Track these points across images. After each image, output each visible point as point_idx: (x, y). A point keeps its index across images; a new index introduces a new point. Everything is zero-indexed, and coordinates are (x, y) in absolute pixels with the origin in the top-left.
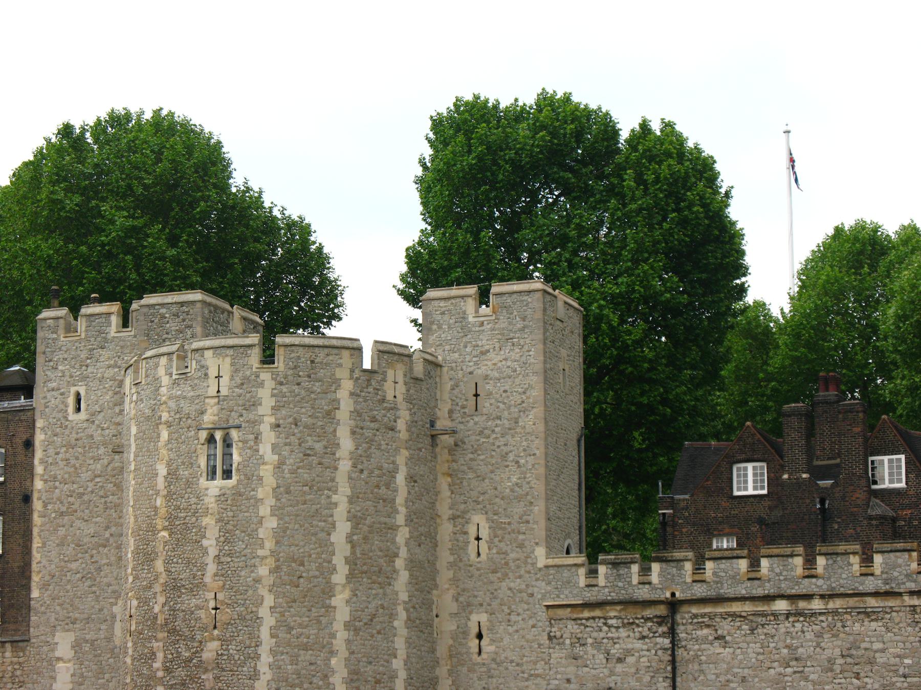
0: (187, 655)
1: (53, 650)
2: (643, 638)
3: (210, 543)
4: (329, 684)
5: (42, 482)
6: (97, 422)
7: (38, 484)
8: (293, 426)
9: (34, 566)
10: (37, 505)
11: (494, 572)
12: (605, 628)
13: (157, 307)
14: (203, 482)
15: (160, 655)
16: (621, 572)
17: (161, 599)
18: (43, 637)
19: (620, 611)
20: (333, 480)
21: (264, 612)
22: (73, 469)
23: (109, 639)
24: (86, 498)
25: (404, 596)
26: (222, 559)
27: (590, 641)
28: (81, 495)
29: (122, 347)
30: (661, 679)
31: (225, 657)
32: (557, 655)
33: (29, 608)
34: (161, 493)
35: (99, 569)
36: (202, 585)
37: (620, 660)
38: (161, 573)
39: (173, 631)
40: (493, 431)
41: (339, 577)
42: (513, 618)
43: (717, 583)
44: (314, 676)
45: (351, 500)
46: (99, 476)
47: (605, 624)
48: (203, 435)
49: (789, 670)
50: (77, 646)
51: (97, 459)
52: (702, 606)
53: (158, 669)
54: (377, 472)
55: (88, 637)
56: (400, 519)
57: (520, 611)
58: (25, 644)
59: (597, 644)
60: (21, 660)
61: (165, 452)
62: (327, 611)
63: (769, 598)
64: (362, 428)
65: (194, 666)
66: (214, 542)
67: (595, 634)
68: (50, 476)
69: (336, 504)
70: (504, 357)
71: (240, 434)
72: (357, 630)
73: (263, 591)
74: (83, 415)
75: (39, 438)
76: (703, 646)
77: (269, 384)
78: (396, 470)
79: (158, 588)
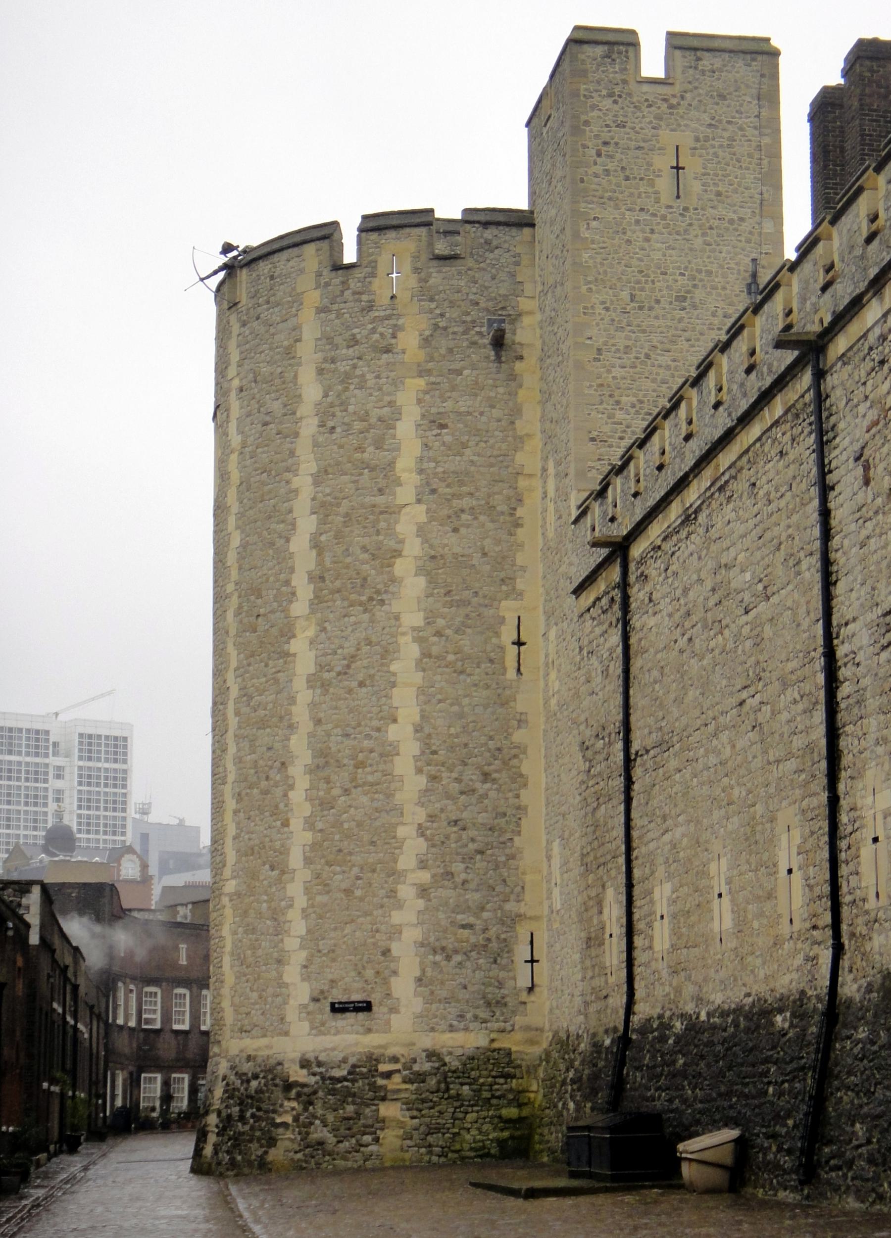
4: (287, 777)
8: (253, 384)
20: (292, 453)
25: (413, 618)
41: (300, 608)
44: (271, 768)
45: (317, 481)
54: (357, 426)
56: (405, 494)
62: (285, 663)
64: (333, 361)
69: (296, 491)
72: (325, 686)
78: (397, 414)
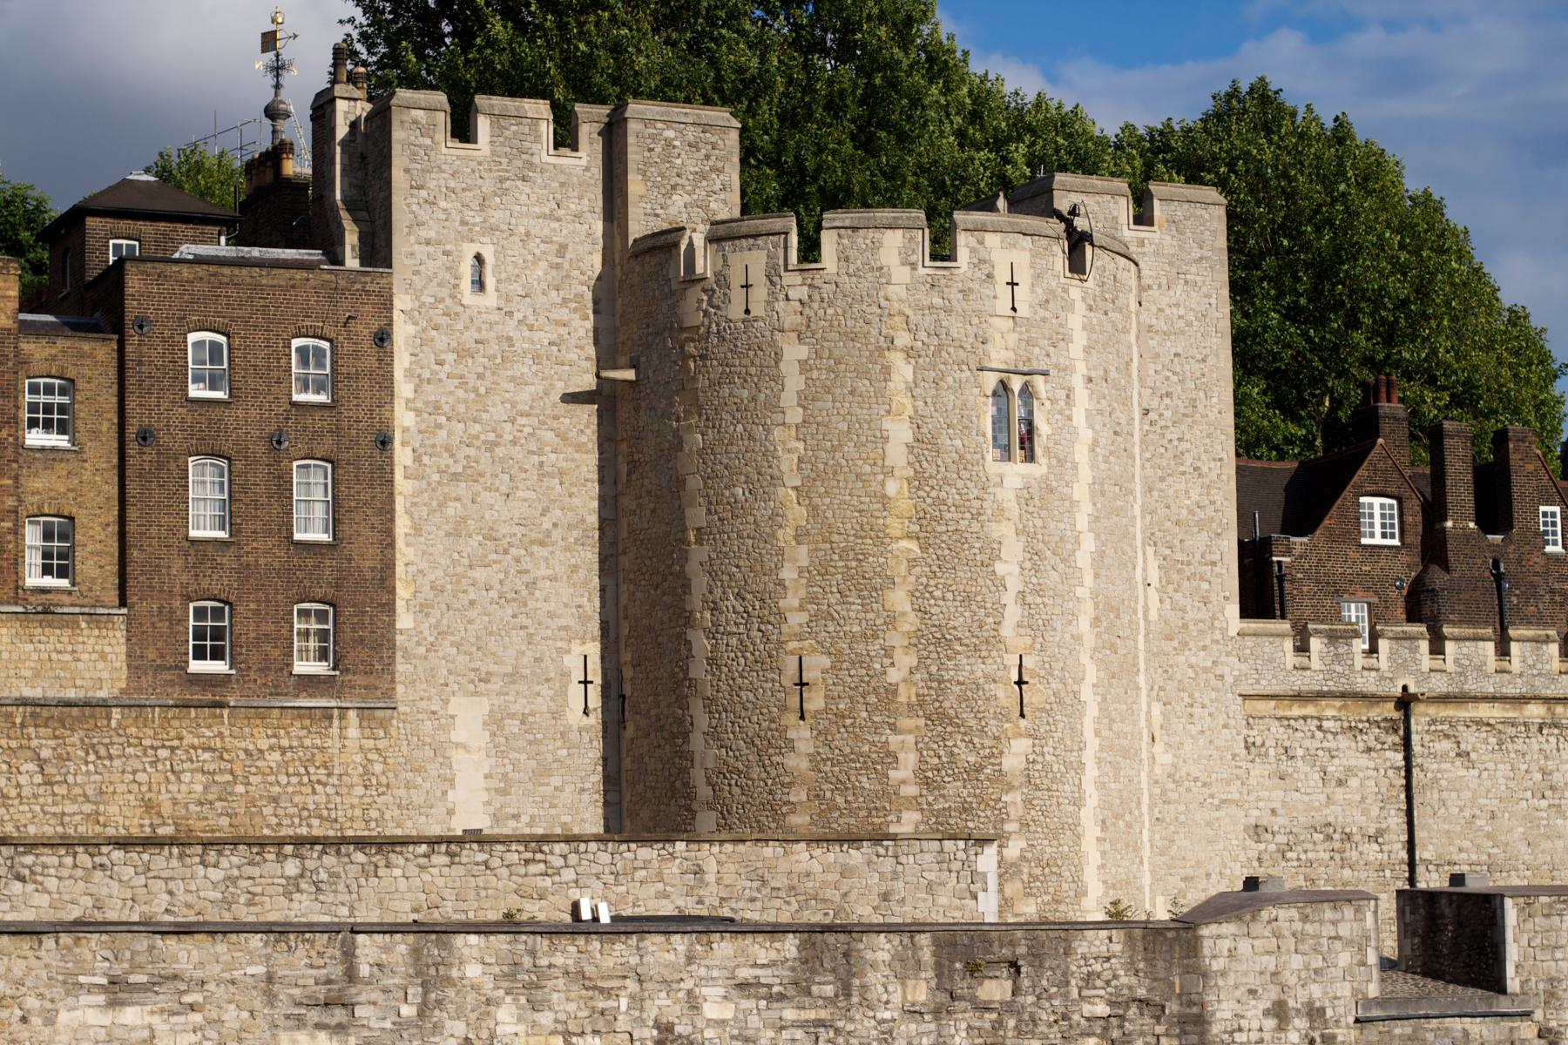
0: (972, 759)
1: (446, 729)
2: (1369, 750)
3: (1009, 568)
5: (412, 414)
6: (518, 316)
7: (403, 419)
9: (400, 569)
10: (402, 455)
11: (1169, 638)
12: (1319, 735)
13: (659, 125)
14: (993, 465)
15: (909, 760)
16: (1341, 651)
17: (906, 660)
18: (423, 704)
19: (1340, 709)
21: (1087, 693)
22: (472, 396)
23: (557, 715)
24: (500, 451)
26: (1029, 599)
27: (1300, 752)
28: (491, 446)
29: (562, 185)
30: (1393, 812)
31: (1039, 767)
32: (1259, 770)
33: (393, 647)
34: (896, 473)
35: (532, 585)
36: (995, 641)
37: (1340, 783)
38: (903, 614)
39: (939, 718)
40: (1161, 415)
42: (1197, 711)
43: (1461, 674)
46: (528, 415)
47: (1320, 728)
48: (991, 381)
49: (1544, 803)
50: (495, 723)
51: (519, 382)
52: (1442, 706)
53: (903, 782)
55: (513, 708)
57: (1207, 701)
58: (389, 712)
59: (1310, 756)
60: (381, 744)
61: (908, 402)
63: (1522, 700)
65: (988, 779)
66: (1017, 570)
67: (1307, 743)
68: (426, 403)
70: (1174, 301)
71: (1049, 387)
73: (1085, 659)
74: (490, 299)
75: (402, 332)
76: (1444, 766)
77: (1080, 307)
79: (896, 639)
